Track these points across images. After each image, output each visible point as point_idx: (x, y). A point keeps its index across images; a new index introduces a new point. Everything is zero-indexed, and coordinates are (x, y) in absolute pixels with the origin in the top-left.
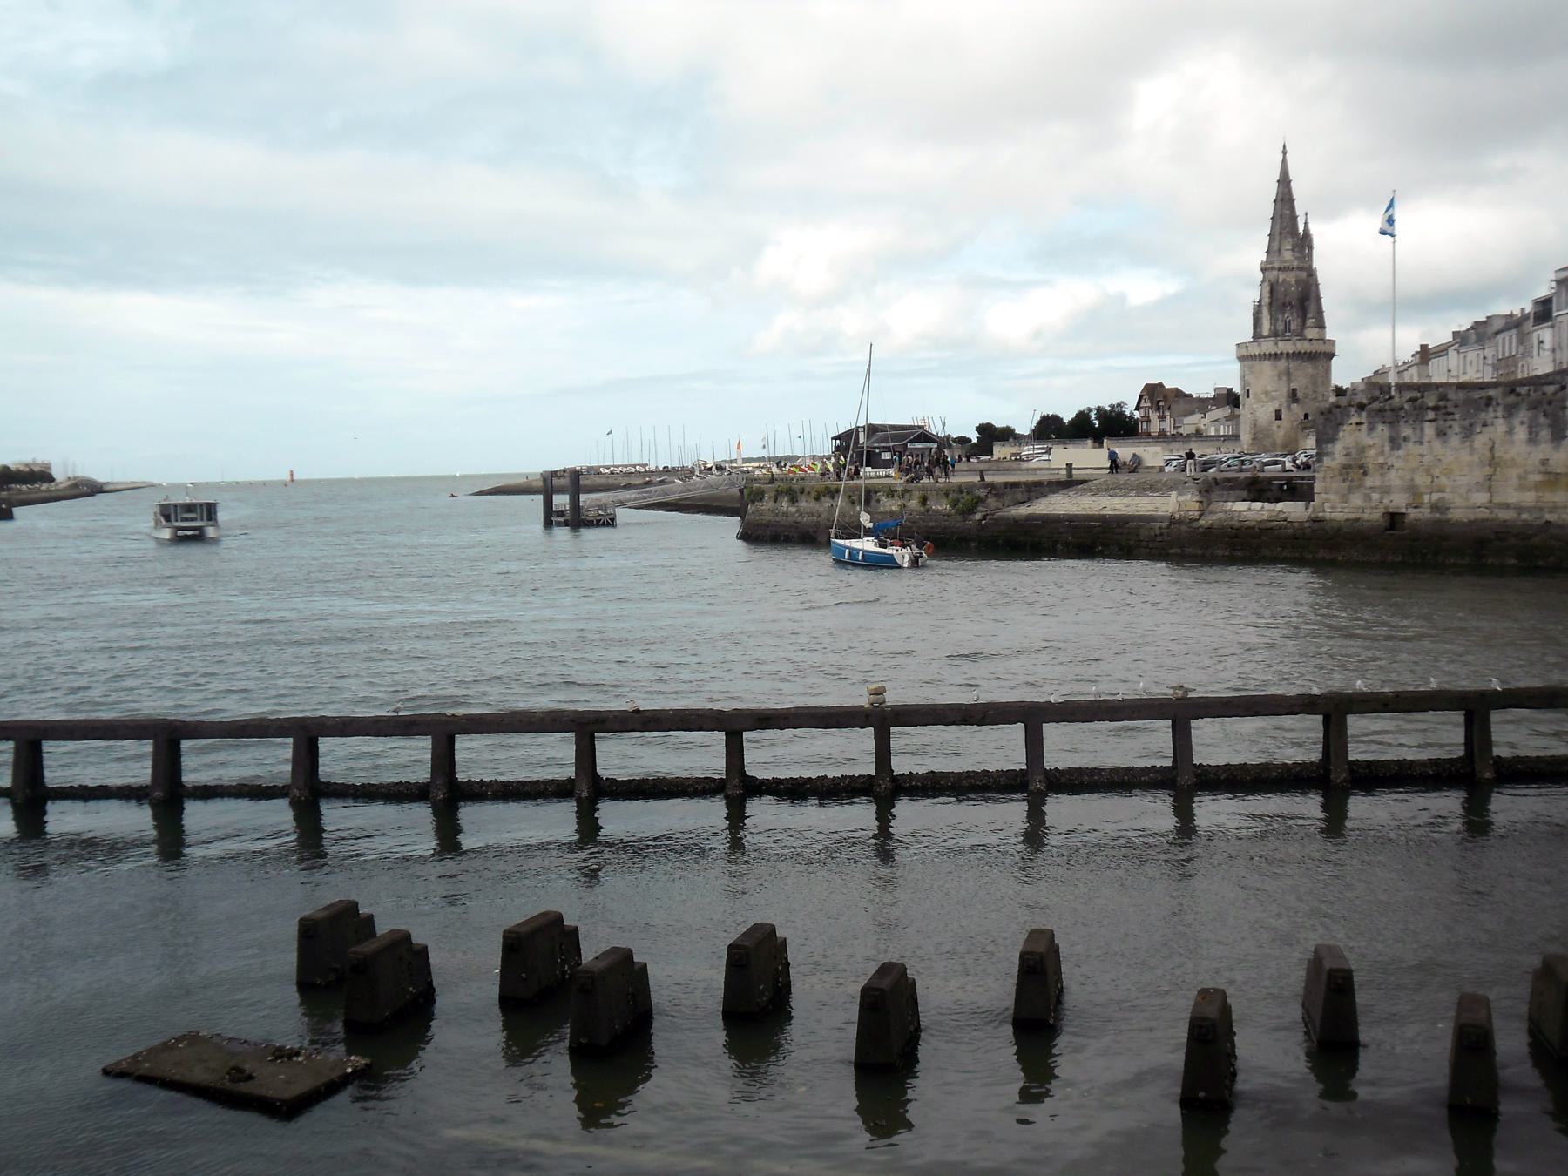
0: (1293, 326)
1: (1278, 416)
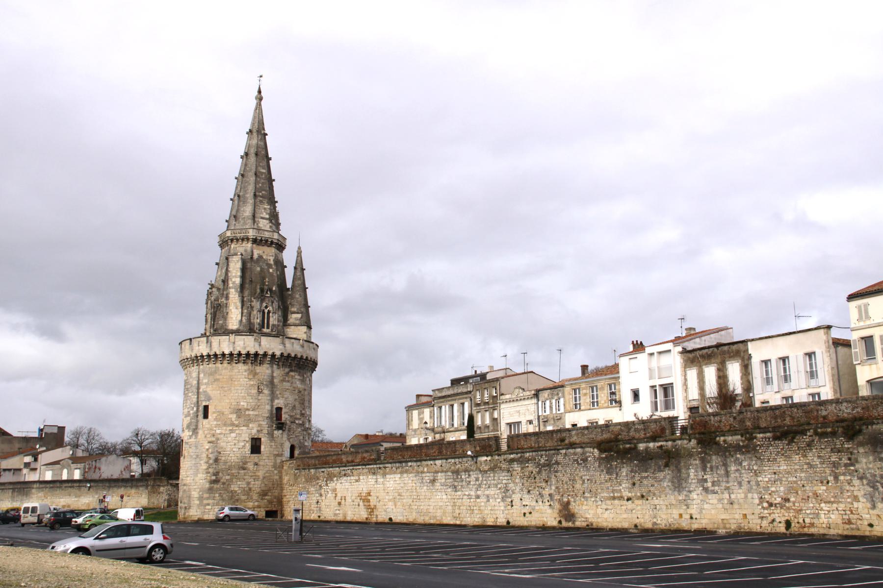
0: (274, 320)
1: (256, 446)
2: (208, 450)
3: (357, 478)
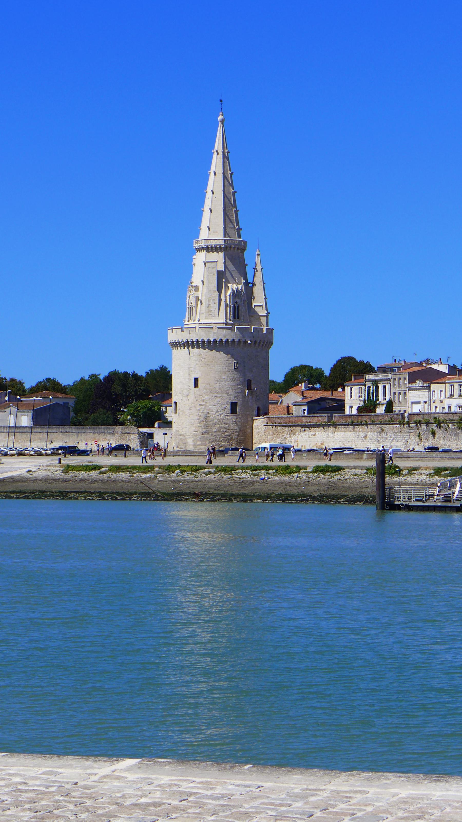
2: (199, 410)
3: (314, 433)
